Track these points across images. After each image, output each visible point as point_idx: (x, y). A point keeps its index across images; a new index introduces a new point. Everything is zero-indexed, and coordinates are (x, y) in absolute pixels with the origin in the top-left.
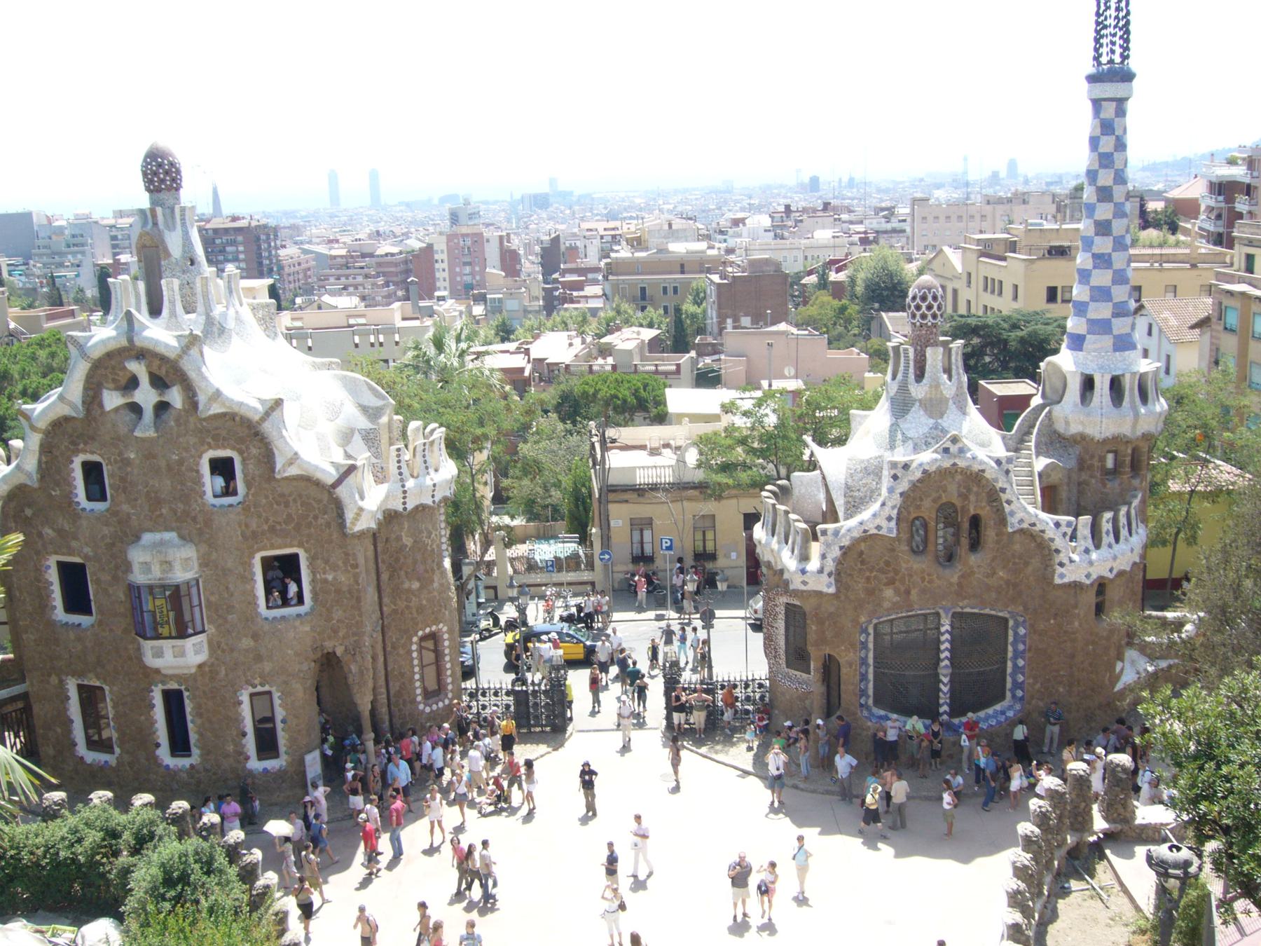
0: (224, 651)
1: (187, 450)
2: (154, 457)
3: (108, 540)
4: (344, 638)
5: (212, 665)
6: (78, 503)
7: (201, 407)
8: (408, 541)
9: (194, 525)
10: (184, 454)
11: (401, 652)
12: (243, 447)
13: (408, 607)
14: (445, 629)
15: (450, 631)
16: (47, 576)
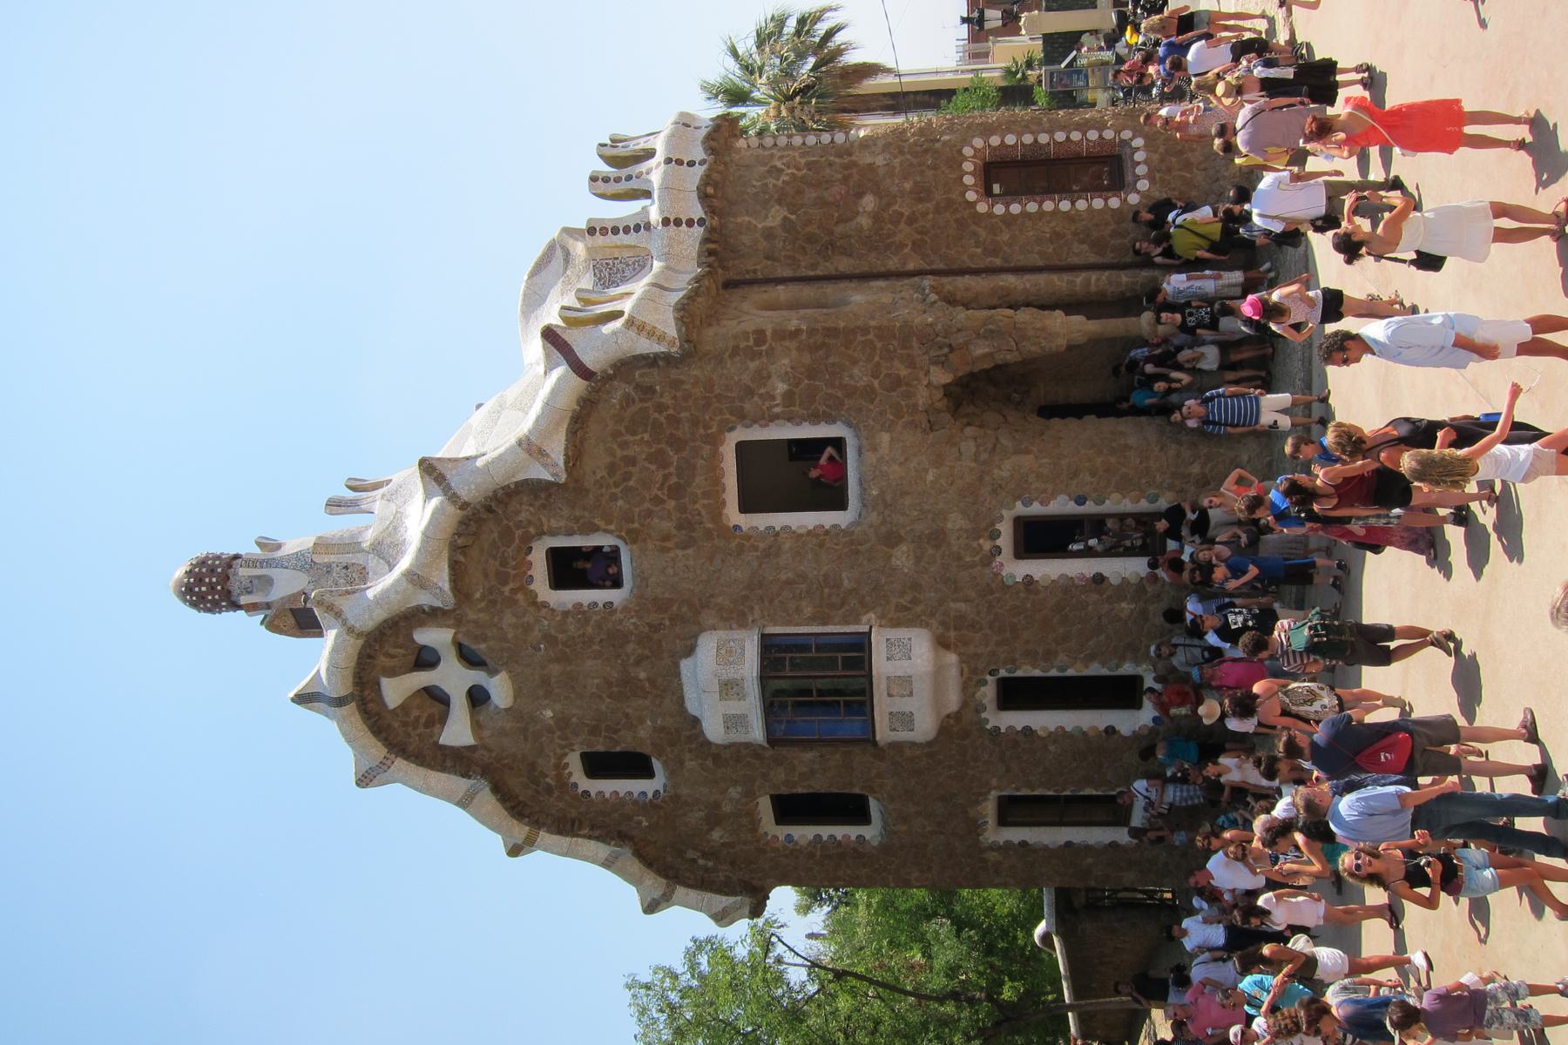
0: (915, 601)
1: (528, 629)
2: (545, 682)
3: (709, 763)
4: (912, 364)
5: (943, 623)
6: (657, 792)
7: (438, 604)
8: (775, 216)
9: (669, 629)
10: (536, 633)
11: (1006, 237)
12: (518, 533)
13: (911, 220)
14: (978, 142)
15: (987, 130)
16: (803, 842)
